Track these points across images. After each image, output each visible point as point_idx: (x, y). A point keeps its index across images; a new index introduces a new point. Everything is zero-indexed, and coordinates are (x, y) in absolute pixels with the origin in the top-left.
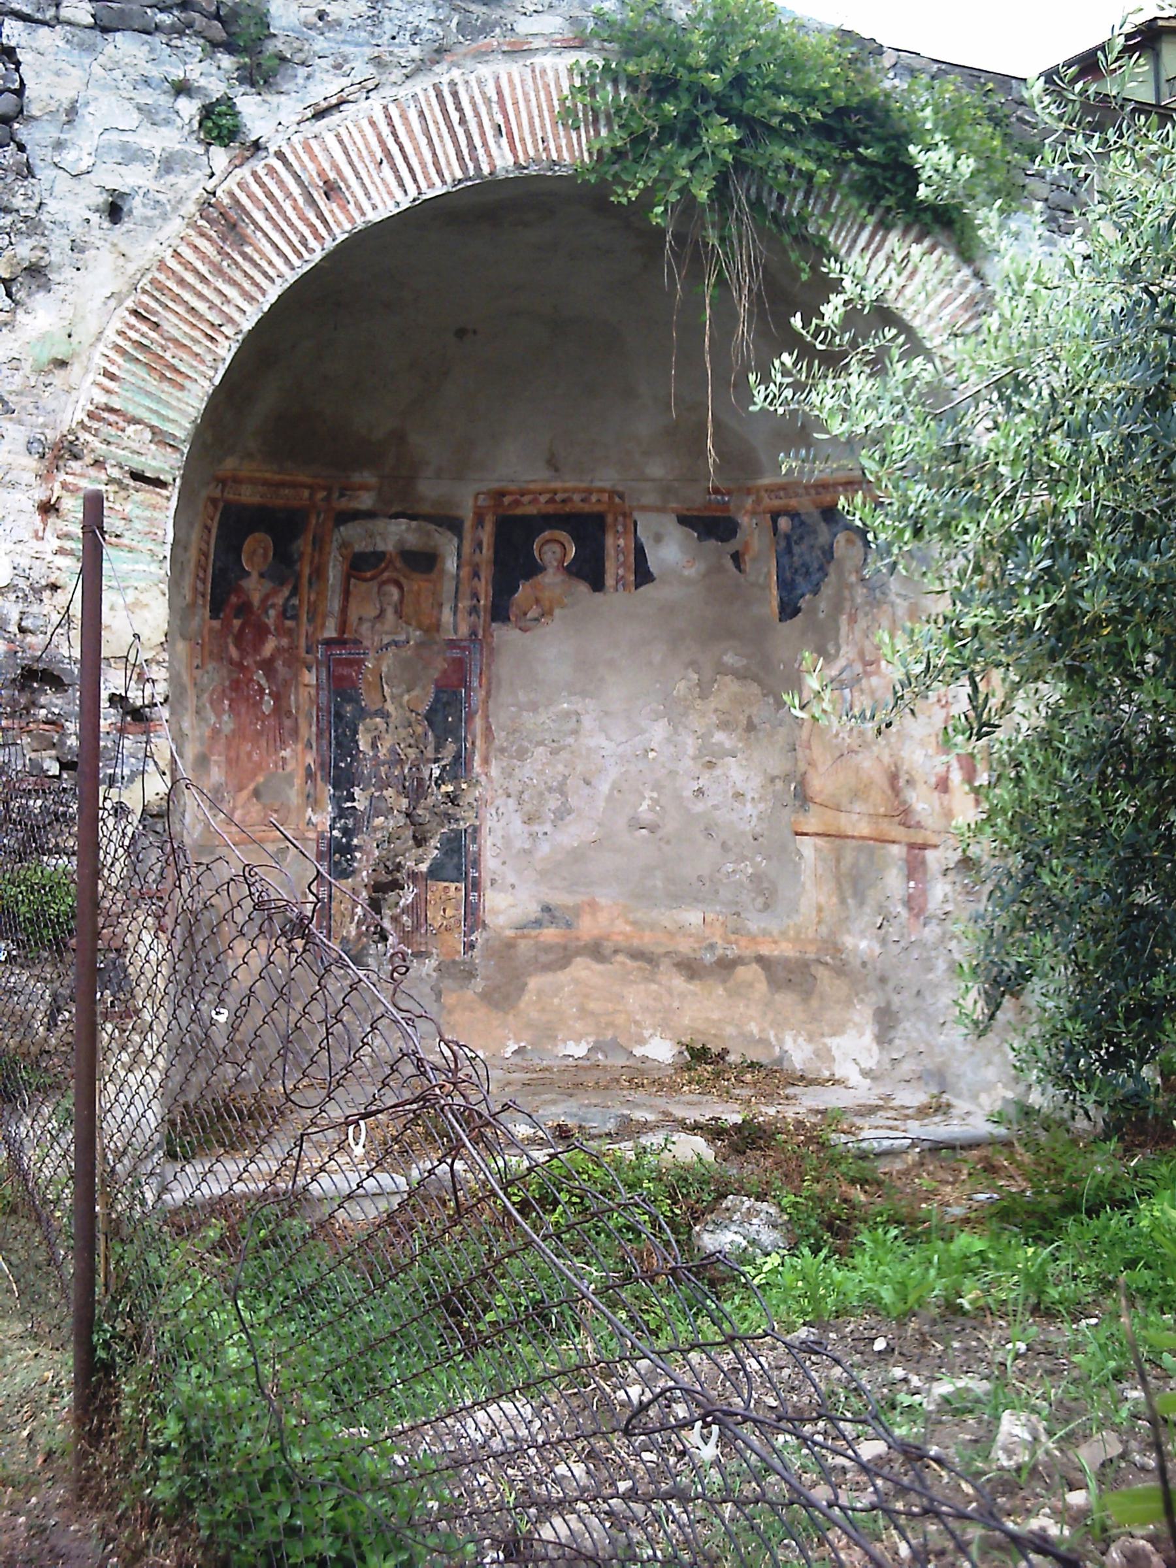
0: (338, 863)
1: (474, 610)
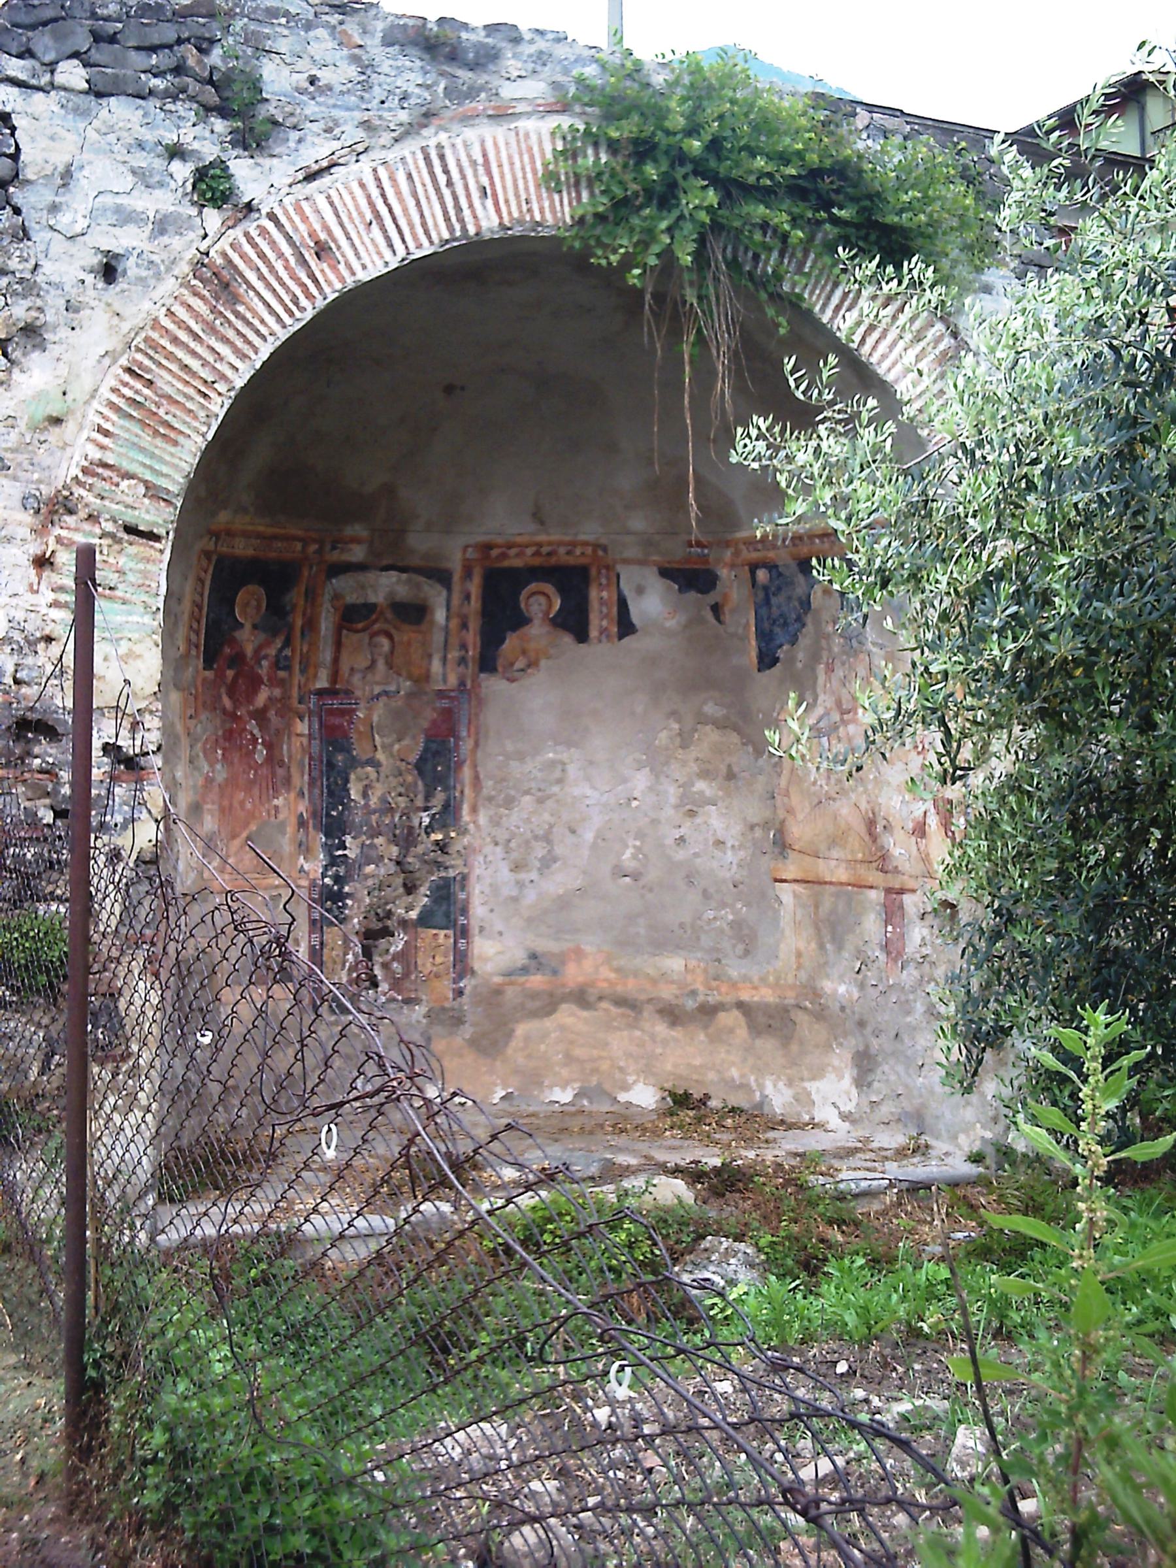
1: (462, 661)
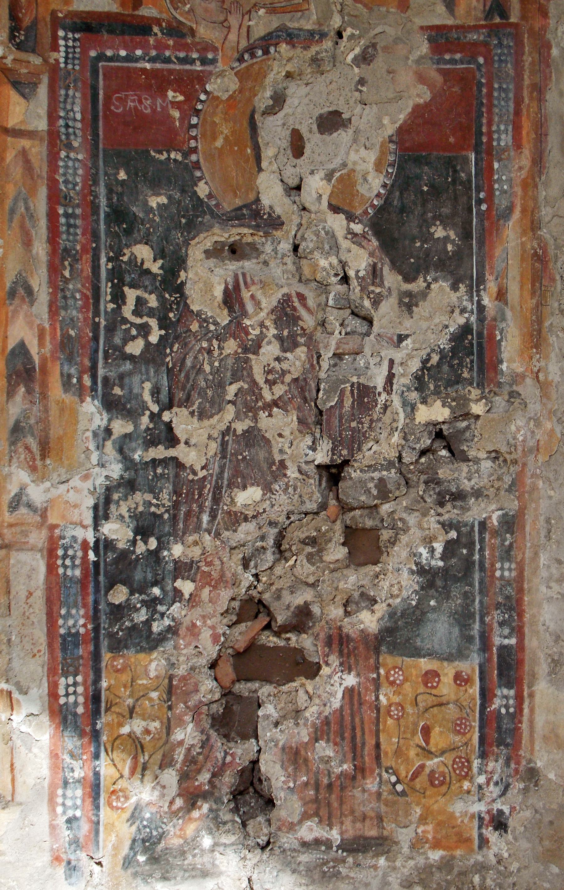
0: (118, 612)
